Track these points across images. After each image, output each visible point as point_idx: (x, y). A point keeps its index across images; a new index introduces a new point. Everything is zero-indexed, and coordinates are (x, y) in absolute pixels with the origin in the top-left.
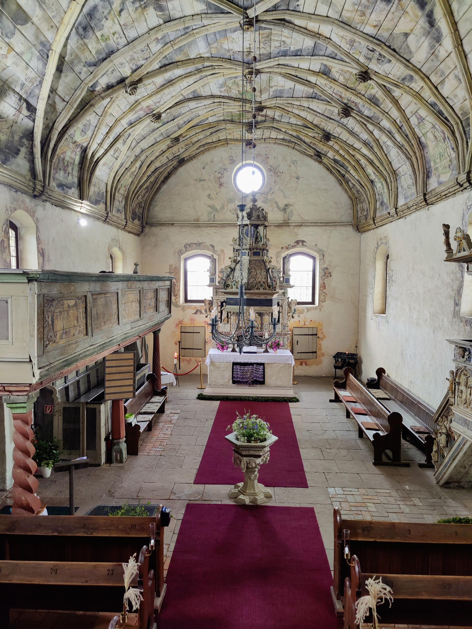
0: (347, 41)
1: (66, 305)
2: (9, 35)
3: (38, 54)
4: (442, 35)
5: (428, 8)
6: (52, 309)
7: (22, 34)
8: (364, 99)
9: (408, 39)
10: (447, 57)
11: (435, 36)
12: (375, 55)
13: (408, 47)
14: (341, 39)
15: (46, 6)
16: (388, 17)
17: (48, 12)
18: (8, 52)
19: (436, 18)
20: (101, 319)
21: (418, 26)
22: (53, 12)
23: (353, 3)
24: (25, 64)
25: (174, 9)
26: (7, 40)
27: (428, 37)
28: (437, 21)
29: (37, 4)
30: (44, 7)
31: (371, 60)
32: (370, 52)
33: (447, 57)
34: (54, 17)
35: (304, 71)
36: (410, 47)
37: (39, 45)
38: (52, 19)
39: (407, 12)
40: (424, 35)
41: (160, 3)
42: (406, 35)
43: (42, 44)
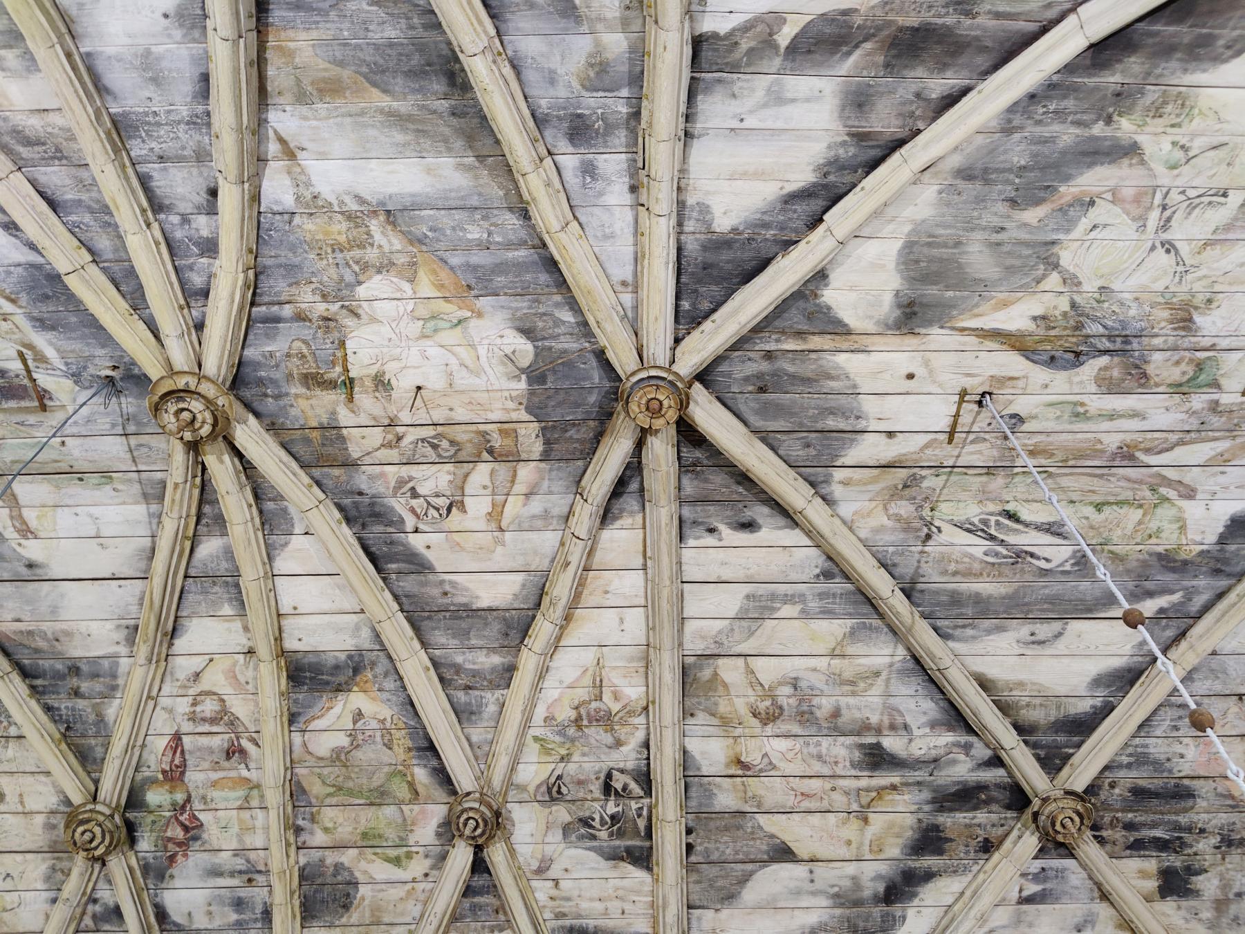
0: (594, 705)
5: (929, 862)
8: (292, 860)
9: (775, 866)
11: (861, 924)
12: (597, 805)
13: (745, 879)
14: (587, 680)
16: (813, 781)
19: (921, 896)
21: (851, 869)
23: (796, 679)
25: (777, 99)
27: (838, 912)
28: (916, 902)
31: (553, 799)
32: (596, 788)
35: (273, 603)
36: (749, 884)
39: (866, 820)
40: (836, 896)
41: (868, 46)
42: (784, 853)
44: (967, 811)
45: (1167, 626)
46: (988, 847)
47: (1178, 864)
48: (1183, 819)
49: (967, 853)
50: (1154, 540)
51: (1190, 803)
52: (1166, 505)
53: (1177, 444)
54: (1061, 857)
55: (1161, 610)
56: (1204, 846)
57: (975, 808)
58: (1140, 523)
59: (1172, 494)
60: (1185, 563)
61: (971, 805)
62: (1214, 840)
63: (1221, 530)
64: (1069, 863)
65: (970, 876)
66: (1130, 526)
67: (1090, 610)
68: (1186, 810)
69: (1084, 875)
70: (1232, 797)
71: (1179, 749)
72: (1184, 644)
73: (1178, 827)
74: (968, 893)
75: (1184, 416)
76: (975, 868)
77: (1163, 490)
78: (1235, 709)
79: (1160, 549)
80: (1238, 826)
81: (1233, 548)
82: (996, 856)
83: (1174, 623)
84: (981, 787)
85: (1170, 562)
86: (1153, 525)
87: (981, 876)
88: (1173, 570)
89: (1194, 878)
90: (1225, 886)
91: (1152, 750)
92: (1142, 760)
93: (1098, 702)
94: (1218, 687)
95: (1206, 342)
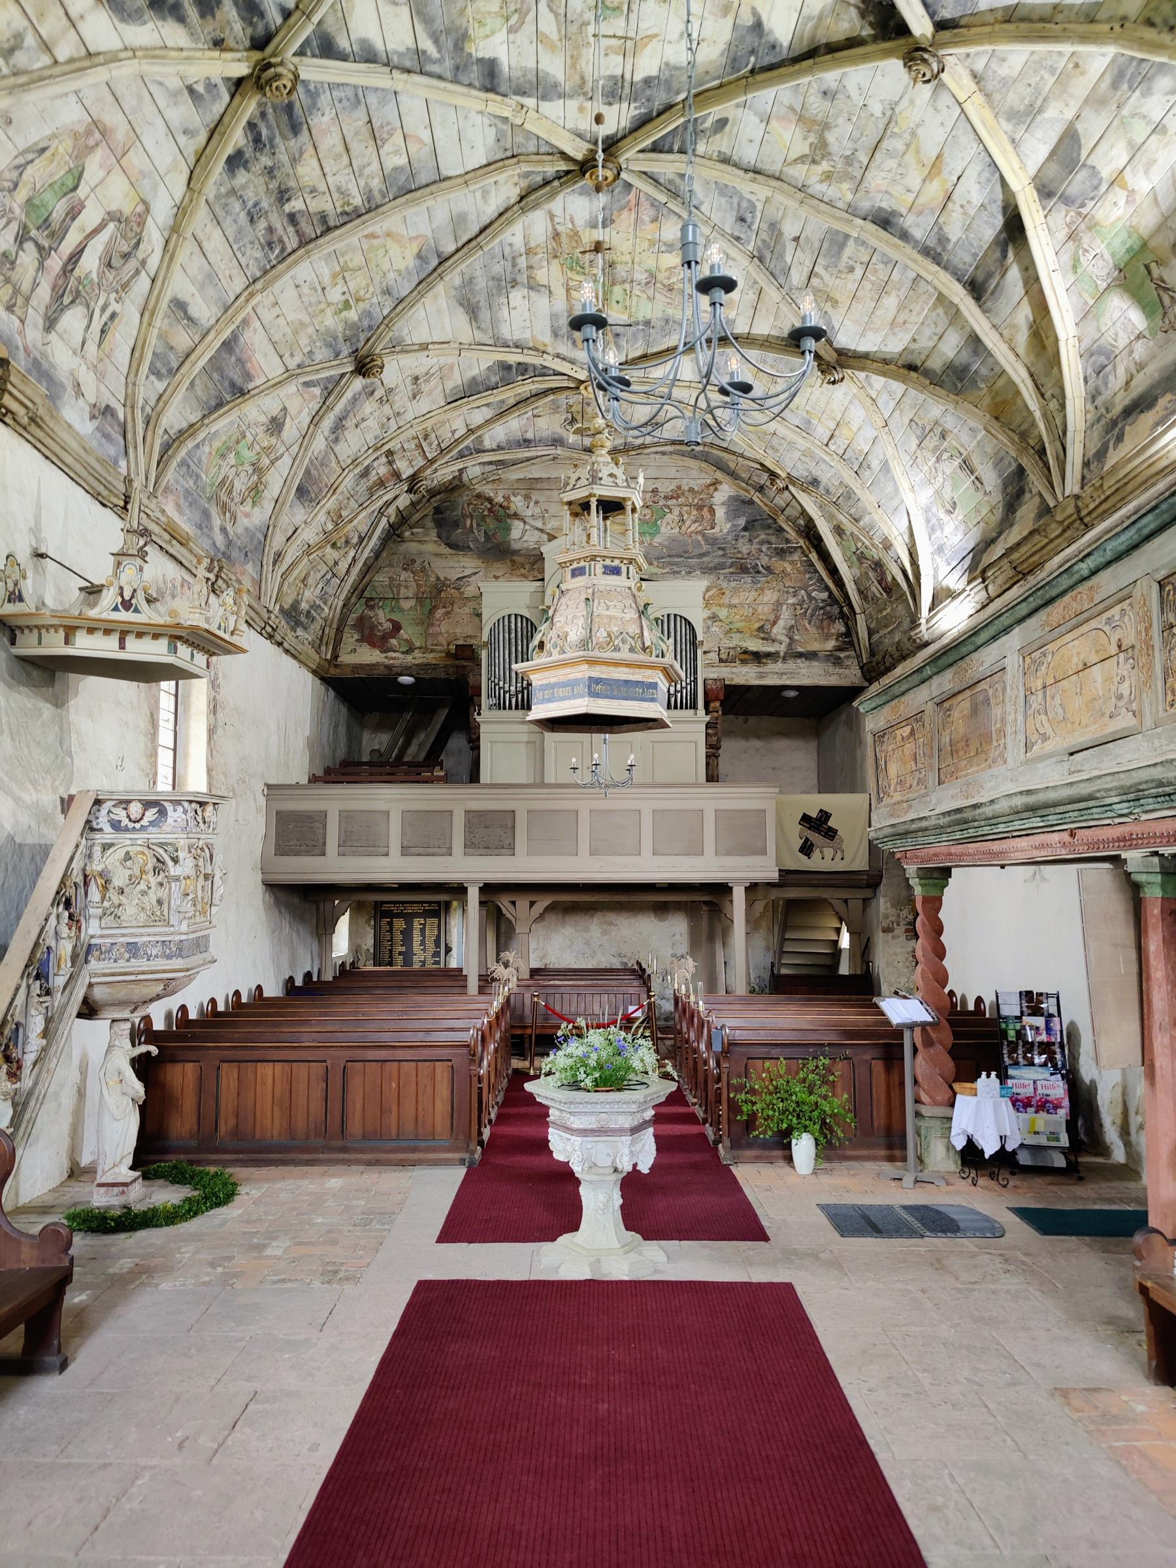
1: (899, 738)
2: (1095, 182)
3: (1137, 93)
4: (123, 20)
6: (884, 746)
7: (1095, 145)
10: (67, 14)
15: (1037, 98)
17: (1047, 89)
18: (1124, 187)
19: (165, 24)
20: (961, 753)
22: (1042, 78)
24: (1153, 137)
26: (1103, 188)
28: (159, 24)
29: (1039, 118)
30: (1039, 102)
33: (67, 14)
34: (1052, 70)
37: (1119, 93)
38: (1058, 72)
43: (1115, 85)
44: (239, 15)
45: (412, 60)
46: (218, 44)
47: (247, 155)
48: (278, 140)
49: (209, 33)
50: (476, 25)
51: (290, 135)
52: (503, 20)
53: (556, 15)
54: (229, 90)
55: (424, 52)
56: (266, 161)
57: (243, 19)
58: (489, 13)
59: (513, 21)
60: (462, 49)
61: (245, 14)
62: (269, 163)
63: (487, 57)
64: (226, 98)
65: (194, 46)
66: (487, 9)
67: (419, 13)
68: (284, 137)
69: (222, 110)
70: (301, 156)
71: (327, 111)
72: (405, 76)
73: (271, 140)
74: (185, 54)
75: (579, 10)
76: (200, 45)
77: (516, 16)
78: (360, 123)
79: (471, 31)
80: (283, 169)
81: (475, 68)
82: (216, 54)
83: (416, 63)
84: (262, 15)
85: (461, 39)
86: (488, 21)
87: (199, 54)
88: (456, 45)
89: (242, 169)
90: (244, 187)
91: (322, 97)
92: (314, 95)
93: (349, 50)
94: (373, 108)
95: (635, 7)
